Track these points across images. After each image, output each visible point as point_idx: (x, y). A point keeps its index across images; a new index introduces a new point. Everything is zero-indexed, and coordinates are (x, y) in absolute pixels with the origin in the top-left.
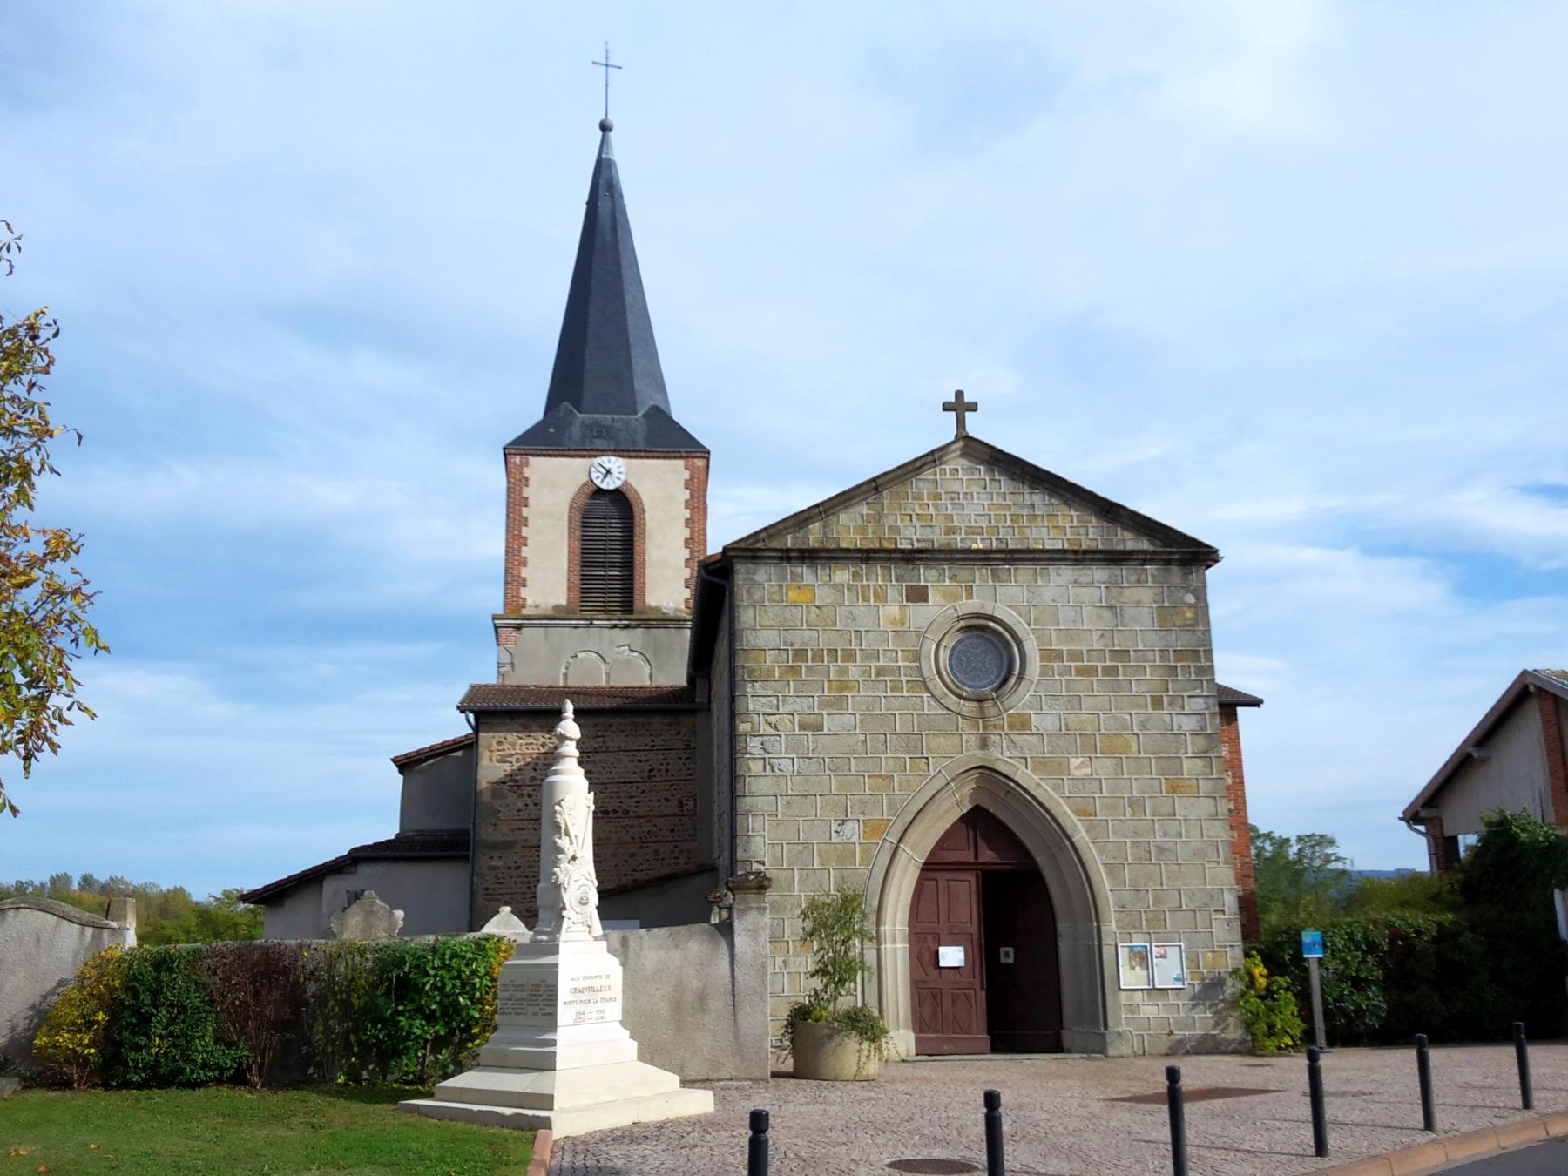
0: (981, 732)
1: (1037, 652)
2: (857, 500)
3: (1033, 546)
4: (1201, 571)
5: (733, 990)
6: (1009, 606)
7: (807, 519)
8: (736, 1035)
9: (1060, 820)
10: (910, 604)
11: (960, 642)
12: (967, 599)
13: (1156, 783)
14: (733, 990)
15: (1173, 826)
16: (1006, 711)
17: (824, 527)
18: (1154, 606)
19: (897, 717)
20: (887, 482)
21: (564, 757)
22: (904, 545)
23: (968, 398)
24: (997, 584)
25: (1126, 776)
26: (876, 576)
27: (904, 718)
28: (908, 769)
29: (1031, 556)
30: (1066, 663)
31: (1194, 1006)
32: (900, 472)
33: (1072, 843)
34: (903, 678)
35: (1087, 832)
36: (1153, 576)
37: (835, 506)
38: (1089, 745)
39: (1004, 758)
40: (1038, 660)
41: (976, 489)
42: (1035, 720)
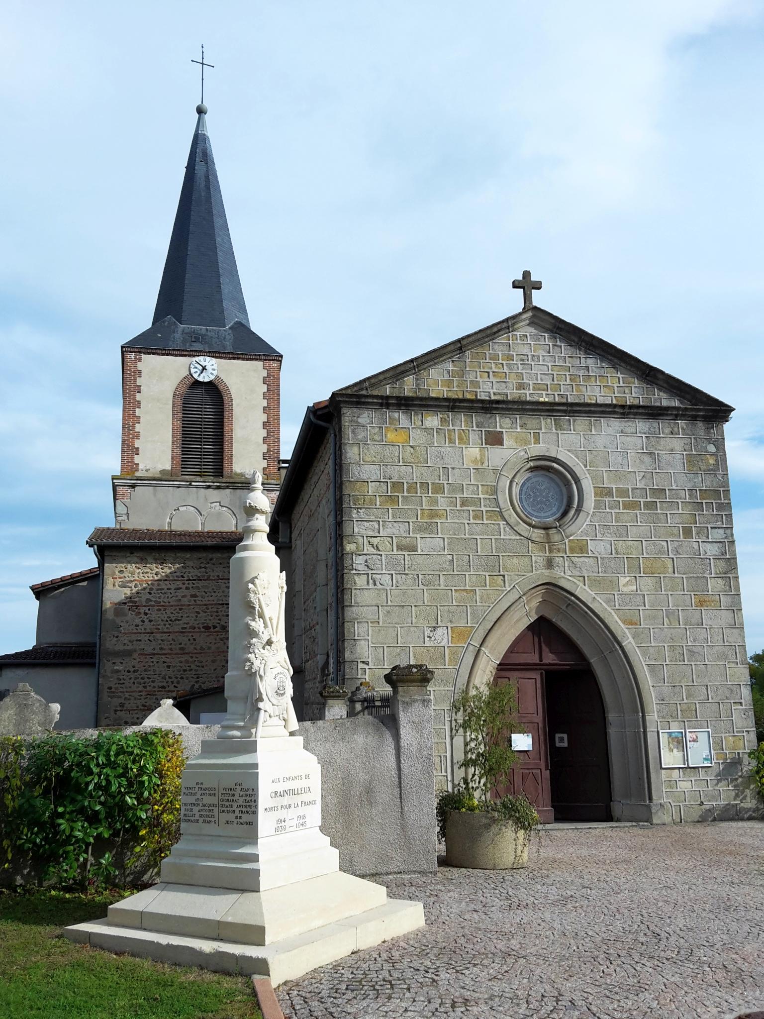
0: (547, 554)
1: (592, 489)
2: (445, 357)
3: (588, 401)
4: (719, 426)
5: (400, 783)
6: (568, 450)
7: (403, 372)
8: (403, 827)
9: (612, 628)
10: (488, 446)
11: (528, 479)
12: (535, 444)
13: (687, 598)
14: (400, 783)
15: (701, 634)
16: (567, 537)
17: (417, 380)
18: (685, 453)
19: (479, 541)
20: (469, 344)
21: (255, 531)
22: (483, 396)
23: (534, 278)
24: (559, 432)
25: (663, 593)
26: (461, 422)
27: (484, 541)
28: (488, 584)
29: (587, 409)
30: (615, 499)
31: (719, 781)
32: (479, 336)
33: (621, 647)
34: (483, 508)
35: (633, 638)
36: (683, 429)
37: (426, 362)
38: (635, 567)
39: (566, 577)
40: (593, 495)
41: (541, 353)
42: (591, 545)
